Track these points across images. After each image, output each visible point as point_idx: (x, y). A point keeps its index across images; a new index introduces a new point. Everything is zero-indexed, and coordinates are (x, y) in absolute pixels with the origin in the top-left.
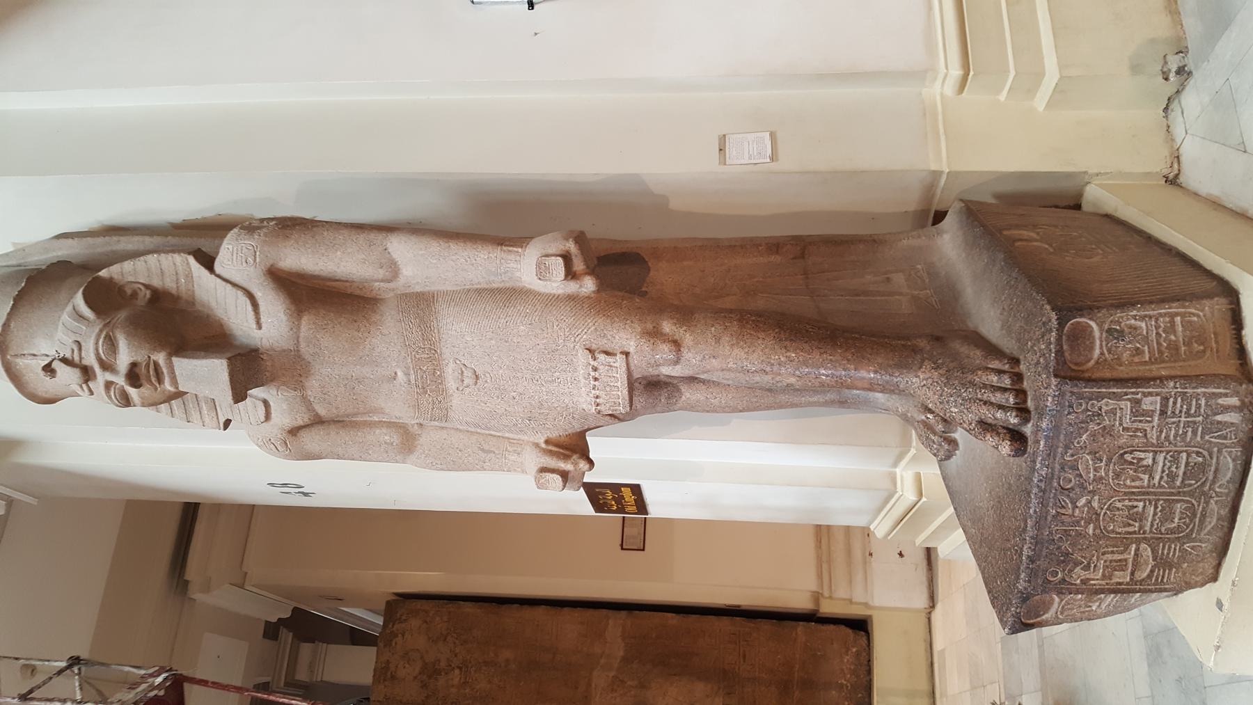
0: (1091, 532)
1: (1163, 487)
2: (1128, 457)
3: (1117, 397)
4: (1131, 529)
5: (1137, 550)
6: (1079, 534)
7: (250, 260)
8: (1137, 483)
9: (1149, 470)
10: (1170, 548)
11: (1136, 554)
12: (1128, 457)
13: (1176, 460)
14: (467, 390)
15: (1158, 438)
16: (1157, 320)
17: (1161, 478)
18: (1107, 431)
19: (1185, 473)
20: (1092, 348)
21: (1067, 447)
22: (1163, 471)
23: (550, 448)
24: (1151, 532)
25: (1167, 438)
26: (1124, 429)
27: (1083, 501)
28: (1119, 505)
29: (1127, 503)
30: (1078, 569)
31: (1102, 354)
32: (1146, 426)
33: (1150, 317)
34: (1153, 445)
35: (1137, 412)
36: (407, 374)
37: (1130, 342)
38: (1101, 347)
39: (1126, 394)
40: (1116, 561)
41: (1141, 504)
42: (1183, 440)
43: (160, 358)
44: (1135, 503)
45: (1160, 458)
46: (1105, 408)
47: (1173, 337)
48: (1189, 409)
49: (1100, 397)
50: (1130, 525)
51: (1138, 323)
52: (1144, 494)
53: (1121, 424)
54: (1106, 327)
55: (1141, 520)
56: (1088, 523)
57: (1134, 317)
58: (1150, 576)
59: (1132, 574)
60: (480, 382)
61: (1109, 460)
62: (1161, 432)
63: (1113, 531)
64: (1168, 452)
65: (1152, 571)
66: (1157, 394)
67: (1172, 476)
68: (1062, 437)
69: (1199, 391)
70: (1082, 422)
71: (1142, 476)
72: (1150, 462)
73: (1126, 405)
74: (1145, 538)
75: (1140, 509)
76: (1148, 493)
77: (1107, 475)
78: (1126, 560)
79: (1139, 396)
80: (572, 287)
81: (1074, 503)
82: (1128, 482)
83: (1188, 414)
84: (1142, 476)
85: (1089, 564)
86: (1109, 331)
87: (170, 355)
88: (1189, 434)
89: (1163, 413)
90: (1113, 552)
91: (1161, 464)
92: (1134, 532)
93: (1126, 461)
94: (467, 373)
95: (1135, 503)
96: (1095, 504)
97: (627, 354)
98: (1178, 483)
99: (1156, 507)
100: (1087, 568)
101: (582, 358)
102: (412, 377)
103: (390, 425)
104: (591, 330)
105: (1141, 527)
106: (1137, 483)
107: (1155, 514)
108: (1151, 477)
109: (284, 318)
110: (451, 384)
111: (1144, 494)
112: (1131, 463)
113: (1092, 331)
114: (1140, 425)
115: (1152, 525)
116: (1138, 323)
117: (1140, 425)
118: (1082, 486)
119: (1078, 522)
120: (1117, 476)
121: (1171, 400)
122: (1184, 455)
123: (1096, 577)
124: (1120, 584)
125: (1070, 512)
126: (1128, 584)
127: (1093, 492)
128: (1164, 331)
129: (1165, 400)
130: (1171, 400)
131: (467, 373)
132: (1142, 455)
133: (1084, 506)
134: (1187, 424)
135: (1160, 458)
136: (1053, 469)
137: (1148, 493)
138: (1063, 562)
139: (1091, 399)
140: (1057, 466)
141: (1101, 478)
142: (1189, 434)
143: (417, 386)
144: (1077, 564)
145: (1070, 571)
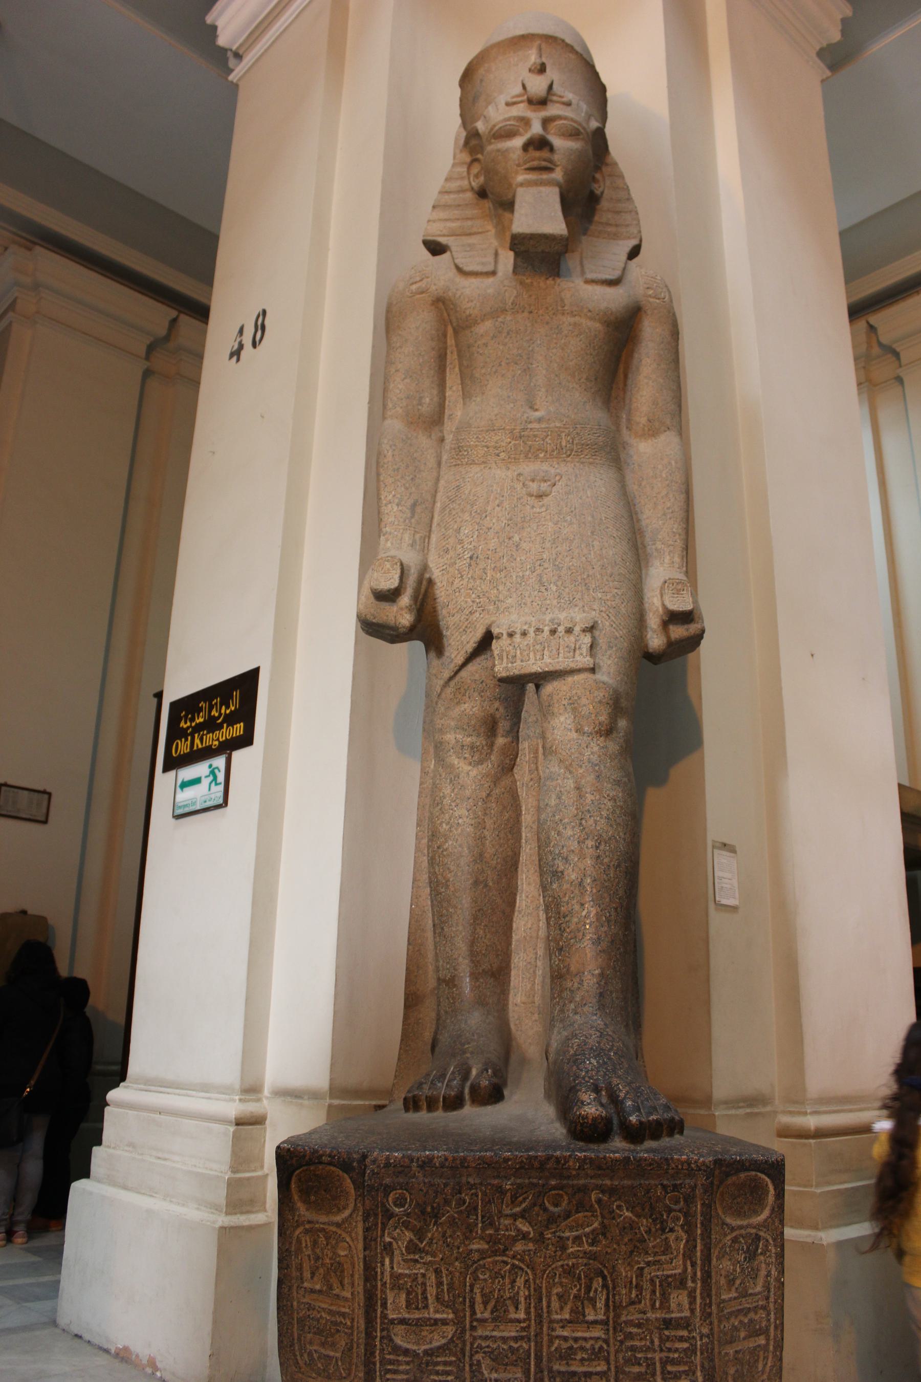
0: (475, 1247)
1: (551, 1342)
2: (598, 1283)
3: (689, 1255)
4: (479, 1307)
5: (444, 1322)
6: (470, 1228)
7: (651, 292)
8: (555, 1304)
9: (578, 1318)
10: (448, 1373)
11: (436, 1321)
12: (598, 1283)
13: (596, 1355)
14: (519, 486)
15: (630, 1323)
16: (764, 1308)
17: (565, 1339)
18: (638, 1246)
19: (574, 1374)
20: (739, 1214)
21: (612, 1191)
22: (576, 1340)
23: (425, 583)
24: (475, 1338)
25: (630, 1336)
26: (642, 1269)
27: (525, 1227)
28: (520, 1282)
29: (523, 1293)
30: (409, 1235)
31: (733, 1229)
32: (646, 1303)
33: (767, 1298)
34: (617, 1316)
35: (668, 1284)
36: (540, 420)
37: (743, 1270)
38: (741, 1227)
39: (693, 1265)
40: (424, 1292)
41: (522, 1315)
42: (628, 1361)
43: (558, 175)
44: (522, 1307)
45: (597, 1332)
46: (672, 1237)
47: (743, 1334)
48: (673, 1362)
49: (689, 1228)
50: (485, 1303)
51: (760, 1281)
52: (539, 1316)
53: (648, 1264)
54: (762, 1234)
55: (495, 1320)
56: (490, 1240)
57: (769, 1274)
58: (396, 1349)
59: (403, 1321)
60: (532, 501)
61: (593, 1256)
62: (639, 1326)
63: (476, 1279)
64: (606, 1341)
65: (406, 1352)
66: (692, 1311)
67: (567, 1355)
68: (627, 1182)
69: (699, 1373)
70: (652, 1208)
71: (567, 1309)
72: (590, 1318)
73: (676, 1268)
74: (463, 1331)
75: (513, 1316)
76: (540, 1323)
77: (569, 1257)
78: (426, 1307)
79: (690, 1284)
80: (653, 621)
81: (522, 1215)
82: (557, 1290)
83: (665, 1362)
84: (567, 1309)
85: (421, 1251)
86: (758, 1238)
87: (558, 184)
88: (636, 1369)
89: (668, 1323)
90: (440, 1284)
91: (587, 1335)
92: (473, 1312)
93: (591, 1280)
94: (544, 487)
95: (522, 1307)
96: (519, 1247)
97: (593, 670)
98: (556, 1367)
99: (516, 1339)
100: (412, 1248)
101: (580, 617)
102: (535, 425)
103: (442, 406)
104: (613, 631)
105: (483, 1321)
106: (555, 1304)
107: (504, 1340)
108: (564, 1324)
109: (603, 305)
110: (528, 468)
111: (539, 1316)
112: (588, 1288)
113: (756, 1213)
114: (647, 1294)
115: (486, 1338)
116: (760, 1281)
117: (647, 1294)
118: (552, 1220)
119: (491, 1224)
120: (569, 1272)
121: (685, 1333)
122: (602, 1367)
123: (395, 1265)
124: (384, 1305)
125: (508, 1211)
126: (384, 1316)
127: (540, 1239)
128: (751, 1321)
129: (686, 1324)
130: (685, 1333)
131: (544, 487)
132: (600, 1304)
133: (519, 1230)
134: (651, 1364)
135: (597, 1332)
136: (577, 1176)
137: (540, 1323)
138: (423, 1212)
139: (686, 1215)
140: (582, 1182)
141: (564, 1248)
142: (636, 1369)
143: (524, 430)
144: (420, 1234)
145: (406, 1225)
